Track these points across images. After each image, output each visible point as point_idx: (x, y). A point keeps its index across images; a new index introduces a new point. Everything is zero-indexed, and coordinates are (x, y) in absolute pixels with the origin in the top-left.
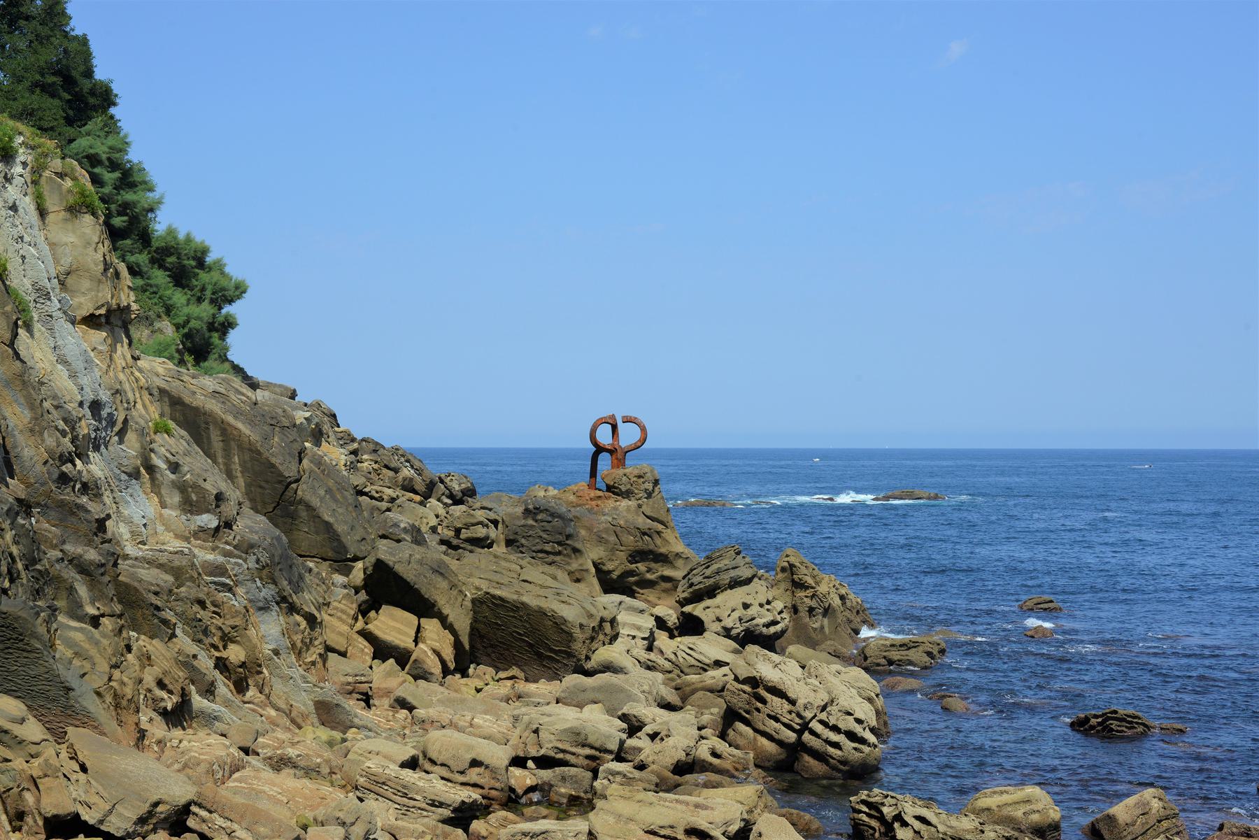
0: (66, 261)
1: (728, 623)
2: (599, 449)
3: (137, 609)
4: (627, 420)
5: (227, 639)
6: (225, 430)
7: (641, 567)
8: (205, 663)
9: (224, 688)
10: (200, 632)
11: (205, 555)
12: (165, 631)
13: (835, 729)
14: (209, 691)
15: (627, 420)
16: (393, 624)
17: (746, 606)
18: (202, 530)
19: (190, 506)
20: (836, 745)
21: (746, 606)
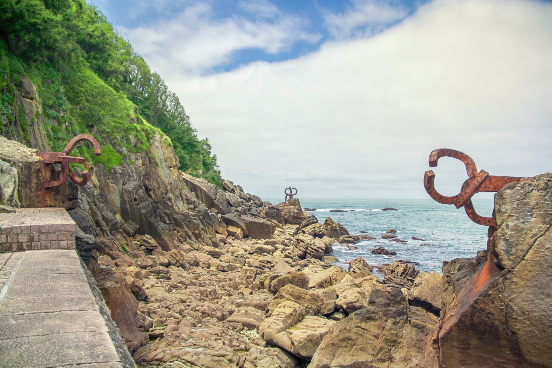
0: (166, 156)
1: (310, 232)
2: (287, 195)
3: (177, 223)
5: (195, 230)
6: (201, 189)
7: (295, 220)
8: (190, 233)
9: (193, 238)
10: (189, 227)
11: (191, 213)
12: (181, 227)
13: (313, 249)
14: (190, 238)
16: (232, 229)
17: (314, 228)
18: (191, 208)
19: (189, 204)
20: (313, 252)
21: (314, 228)
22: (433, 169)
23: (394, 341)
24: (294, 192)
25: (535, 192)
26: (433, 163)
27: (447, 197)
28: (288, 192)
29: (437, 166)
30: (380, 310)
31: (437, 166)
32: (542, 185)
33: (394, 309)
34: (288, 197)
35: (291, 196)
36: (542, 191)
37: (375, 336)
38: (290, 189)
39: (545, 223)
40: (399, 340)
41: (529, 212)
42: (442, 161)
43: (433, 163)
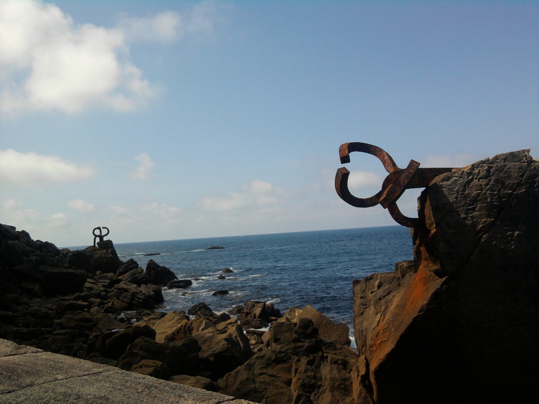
2: (96, 236)
4: (103, 228)
15: (103, 228)
22: (346, 165)
23: (314, 384)
24: (104, 232)
25: (475, 181)
26: (345, 159)
27: (367, 199)
28: (97, 232)
29: (349, 162)
30: (287, 347)
31: (349, 162)
32: (482, 174)
33: (306, 344)
34: (98, 240)
35: (101, 237)
36: (484, 180)
37: (286, 383)
38: (99, 228)
39: (488, 216)
40: (319, 383)
41: (470, 205)
42: (354, 155)
43: (345, 159)
